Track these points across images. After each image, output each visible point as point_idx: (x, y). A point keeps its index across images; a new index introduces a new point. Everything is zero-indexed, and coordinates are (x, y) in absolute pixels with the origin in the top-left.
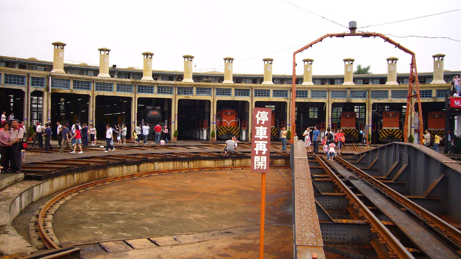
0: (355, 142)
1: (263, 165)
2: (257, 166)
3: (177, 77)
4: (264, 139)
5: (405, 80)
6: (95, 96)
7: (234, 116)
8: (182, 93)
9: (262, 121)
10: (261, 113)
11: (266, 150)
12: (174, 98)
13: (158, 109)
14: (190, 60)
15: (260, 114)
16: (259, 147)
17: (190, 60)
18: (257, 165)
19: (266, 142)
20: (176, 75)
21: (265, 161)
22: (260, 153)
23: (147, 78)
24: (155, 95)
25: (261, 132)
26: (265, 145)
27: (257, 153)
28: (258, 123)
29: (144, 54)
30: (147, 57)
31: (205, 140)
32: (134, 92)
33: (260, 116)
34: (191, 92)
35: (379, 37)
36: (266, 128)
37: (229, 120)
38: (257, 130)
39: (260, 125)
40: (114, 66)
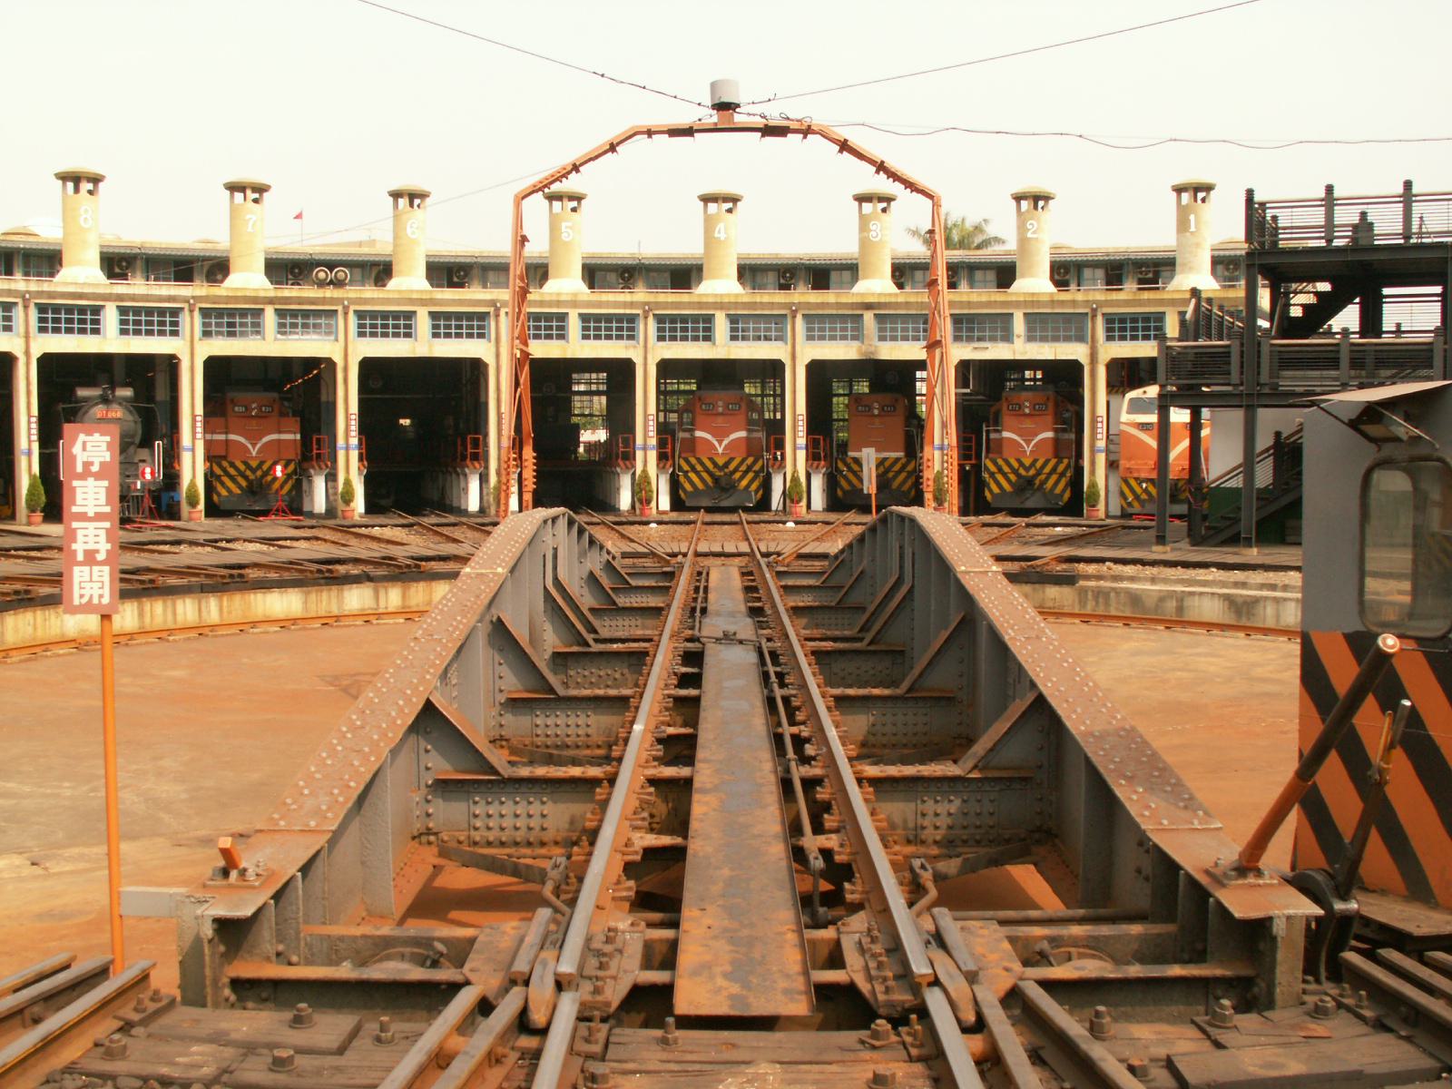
0: (747, 510)
1: (100, 592)
2: (82, 596)
3: (207, 264)
4: (99, 517)
5: (1087, 273)
8: (219, 333)
11: (109, 546)
12: (188, 351)
13: (126, 399)
14: (256, 201)
15: (84, 443)
16: (86, 539)
17: (256, 201)
18: (83, 592)
19: (107, 525)
20: (205, 259)
21: (107, 579)
22: (90, 558)
23: (81, 275)
24: (111, 340)
25: (91, 496)
26: (103, 534)
27: (80, 557)
28: (79, 469)
29: (64, 177)
30: (77, 190)
31: (319, 516)
32: (22, 330)
33: (84, 449)
34: (257, 328)
35: (818, 136)
36: (106, 483)
38: (79, 491)
39: (87, 473)
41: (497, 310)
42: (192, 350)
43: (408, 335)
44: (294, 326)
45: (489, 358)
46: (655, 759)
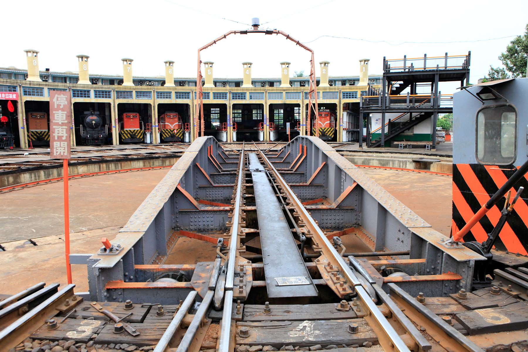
2: (57, 152)
4: (63, 124)
5: (337, 82)
6: (24, 101)
7: (177, 119)
9: (60, 105)
10: (59, 96)
11: (67, 135)
15: (57, 98)
20: (117, 79)
22: (60, 139)
24: (92, 99)
25: (60, 117)
27: (56, 138)
28: (56, 107)
29: (79, 57)
30: (82, 60)
33: (57, 100)
34: (131, 96)
37: (172, 123)
38: (56, 115)
39: (58, 109)
40: (48, 70)
41: (192, 91)
42: (114, 101)
43: (170, 98)
44: (140, 95)
45: (190, 104)
46: (244, 204)
